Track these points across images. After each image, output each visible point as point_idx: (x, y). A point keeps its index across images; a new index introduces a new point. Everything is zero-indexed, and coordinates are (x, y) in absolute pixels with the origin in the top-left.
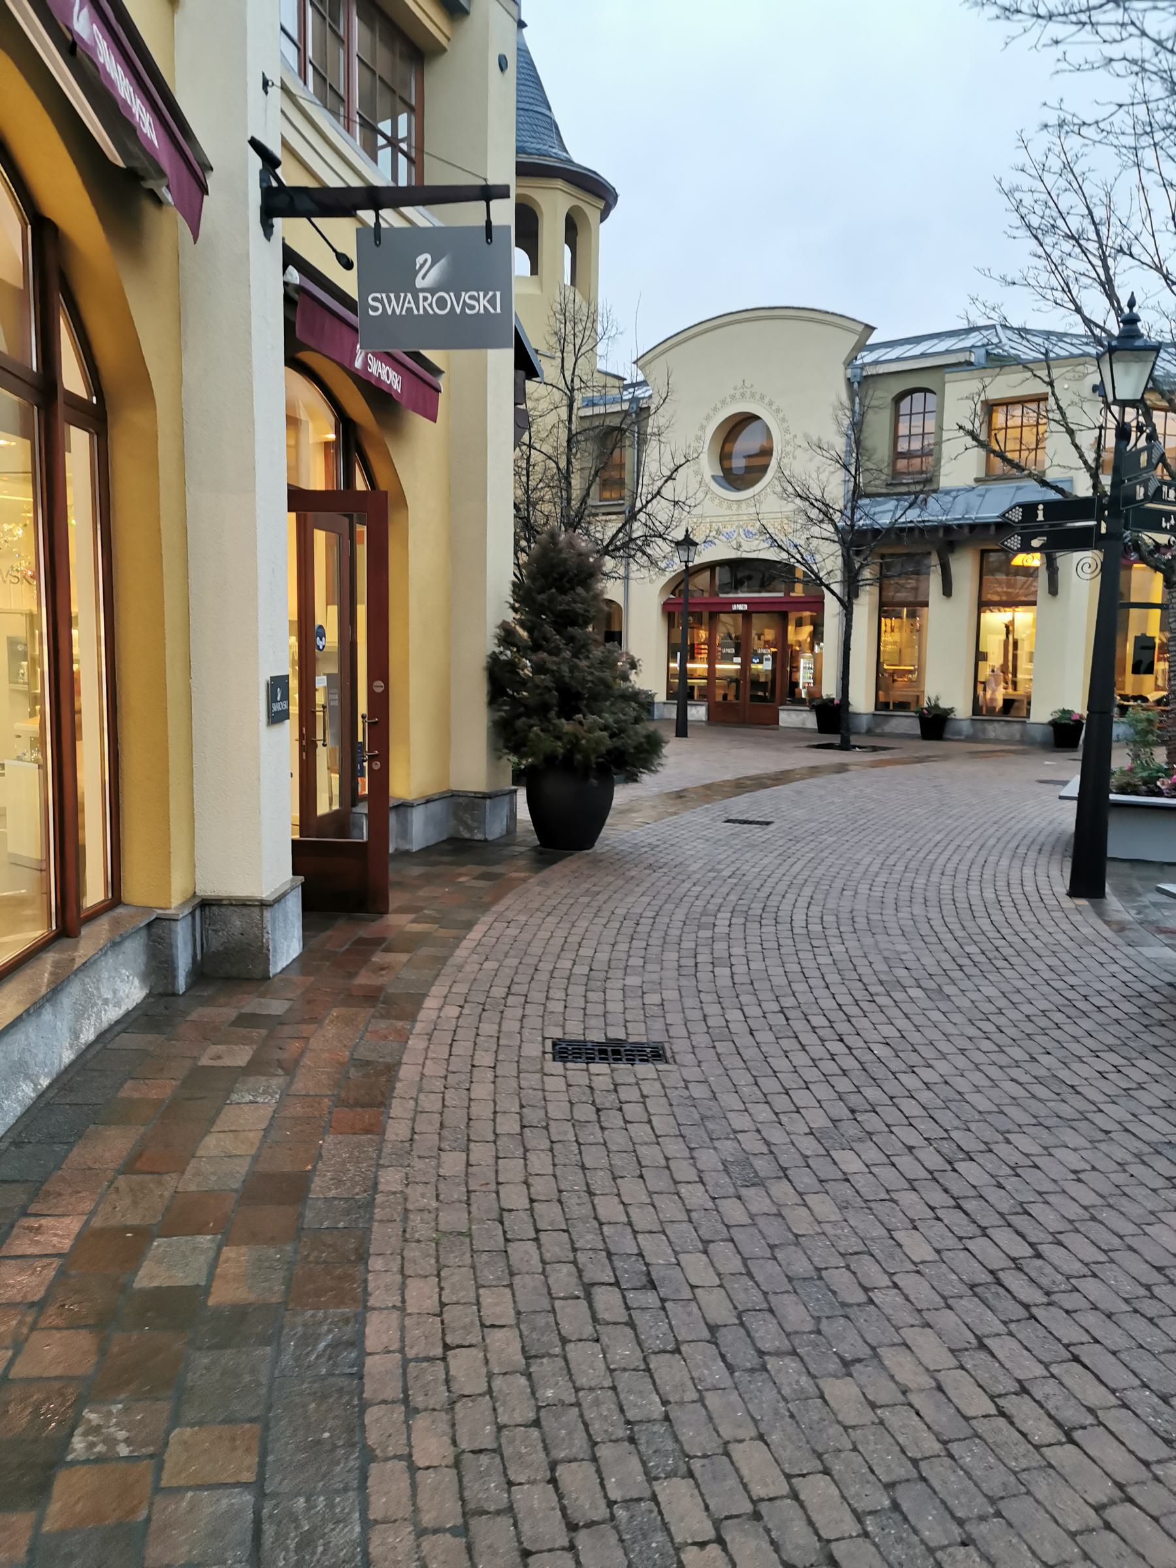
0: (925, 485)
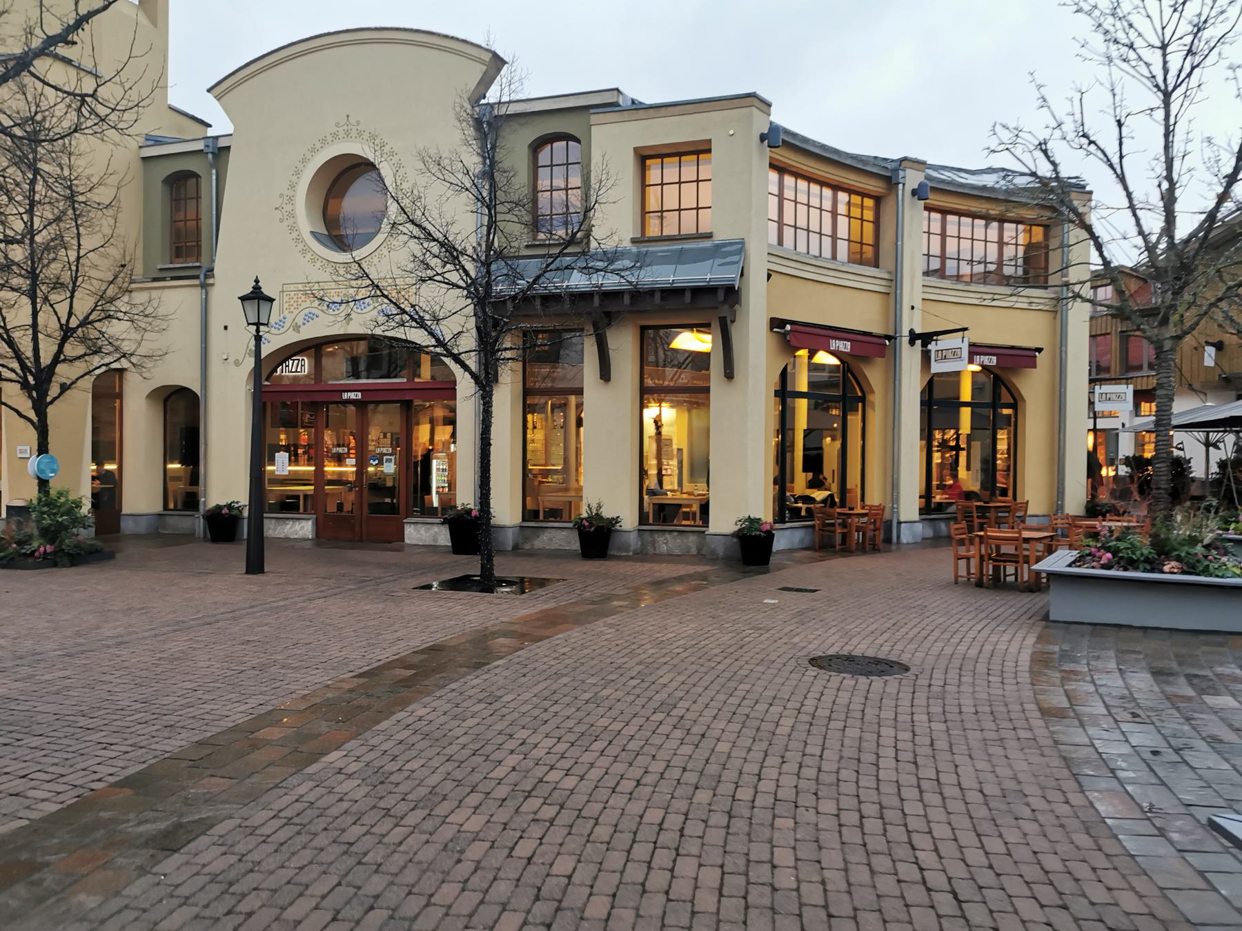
0: (577, 242)
